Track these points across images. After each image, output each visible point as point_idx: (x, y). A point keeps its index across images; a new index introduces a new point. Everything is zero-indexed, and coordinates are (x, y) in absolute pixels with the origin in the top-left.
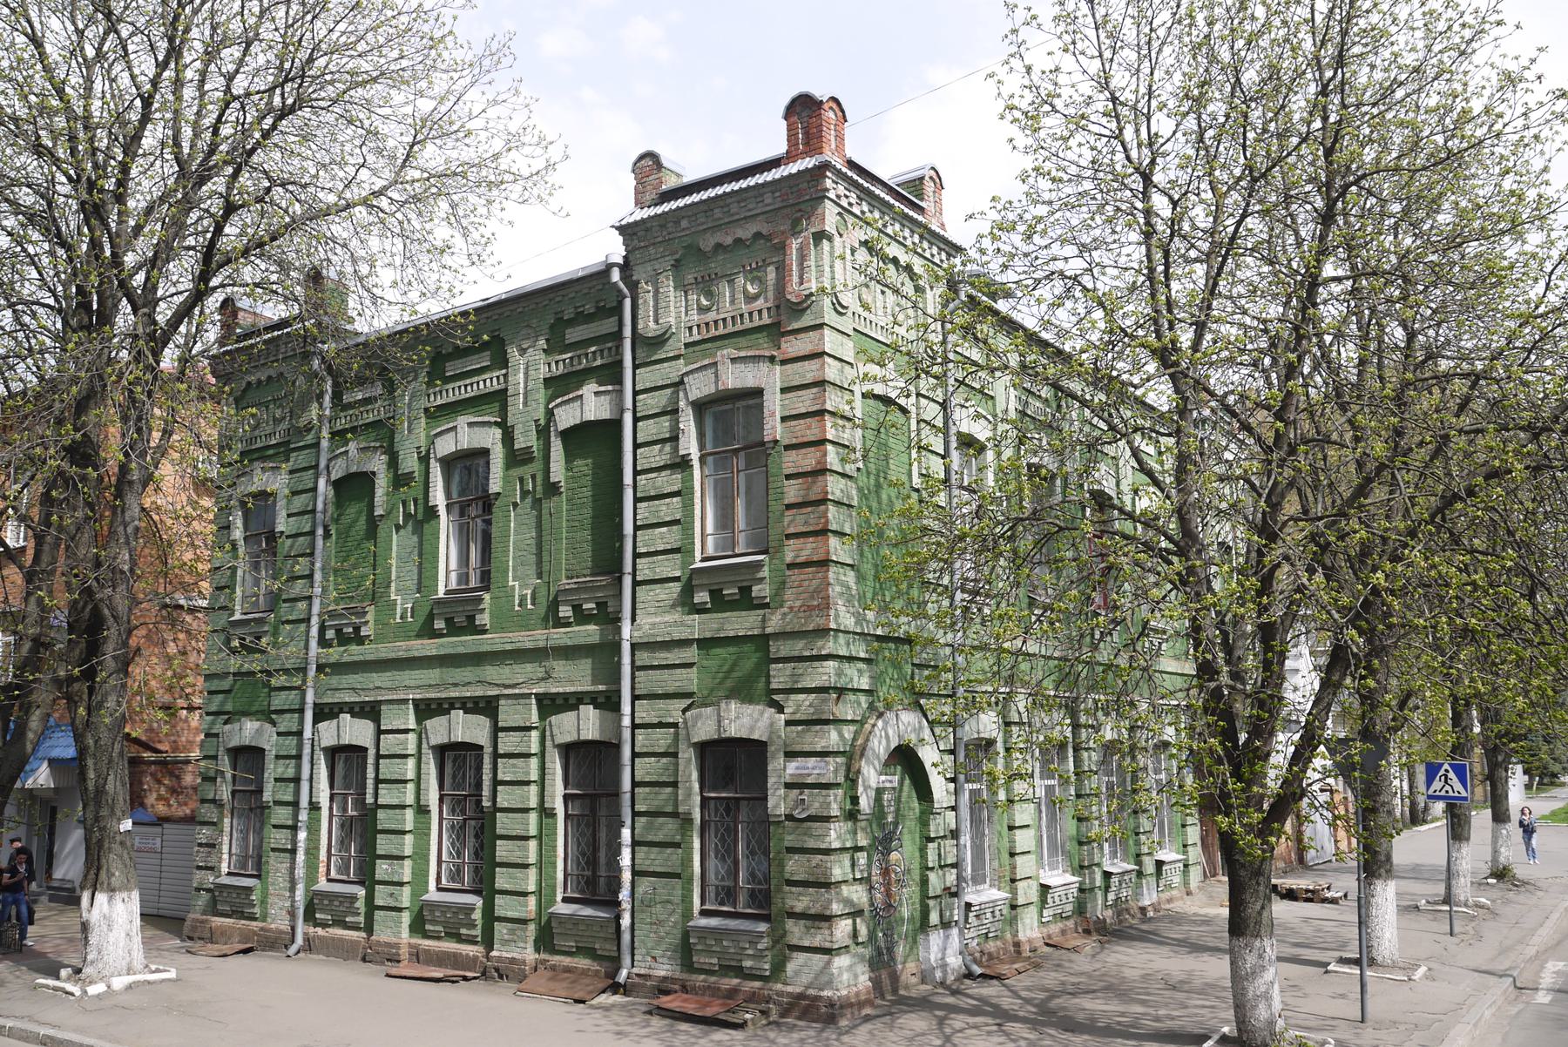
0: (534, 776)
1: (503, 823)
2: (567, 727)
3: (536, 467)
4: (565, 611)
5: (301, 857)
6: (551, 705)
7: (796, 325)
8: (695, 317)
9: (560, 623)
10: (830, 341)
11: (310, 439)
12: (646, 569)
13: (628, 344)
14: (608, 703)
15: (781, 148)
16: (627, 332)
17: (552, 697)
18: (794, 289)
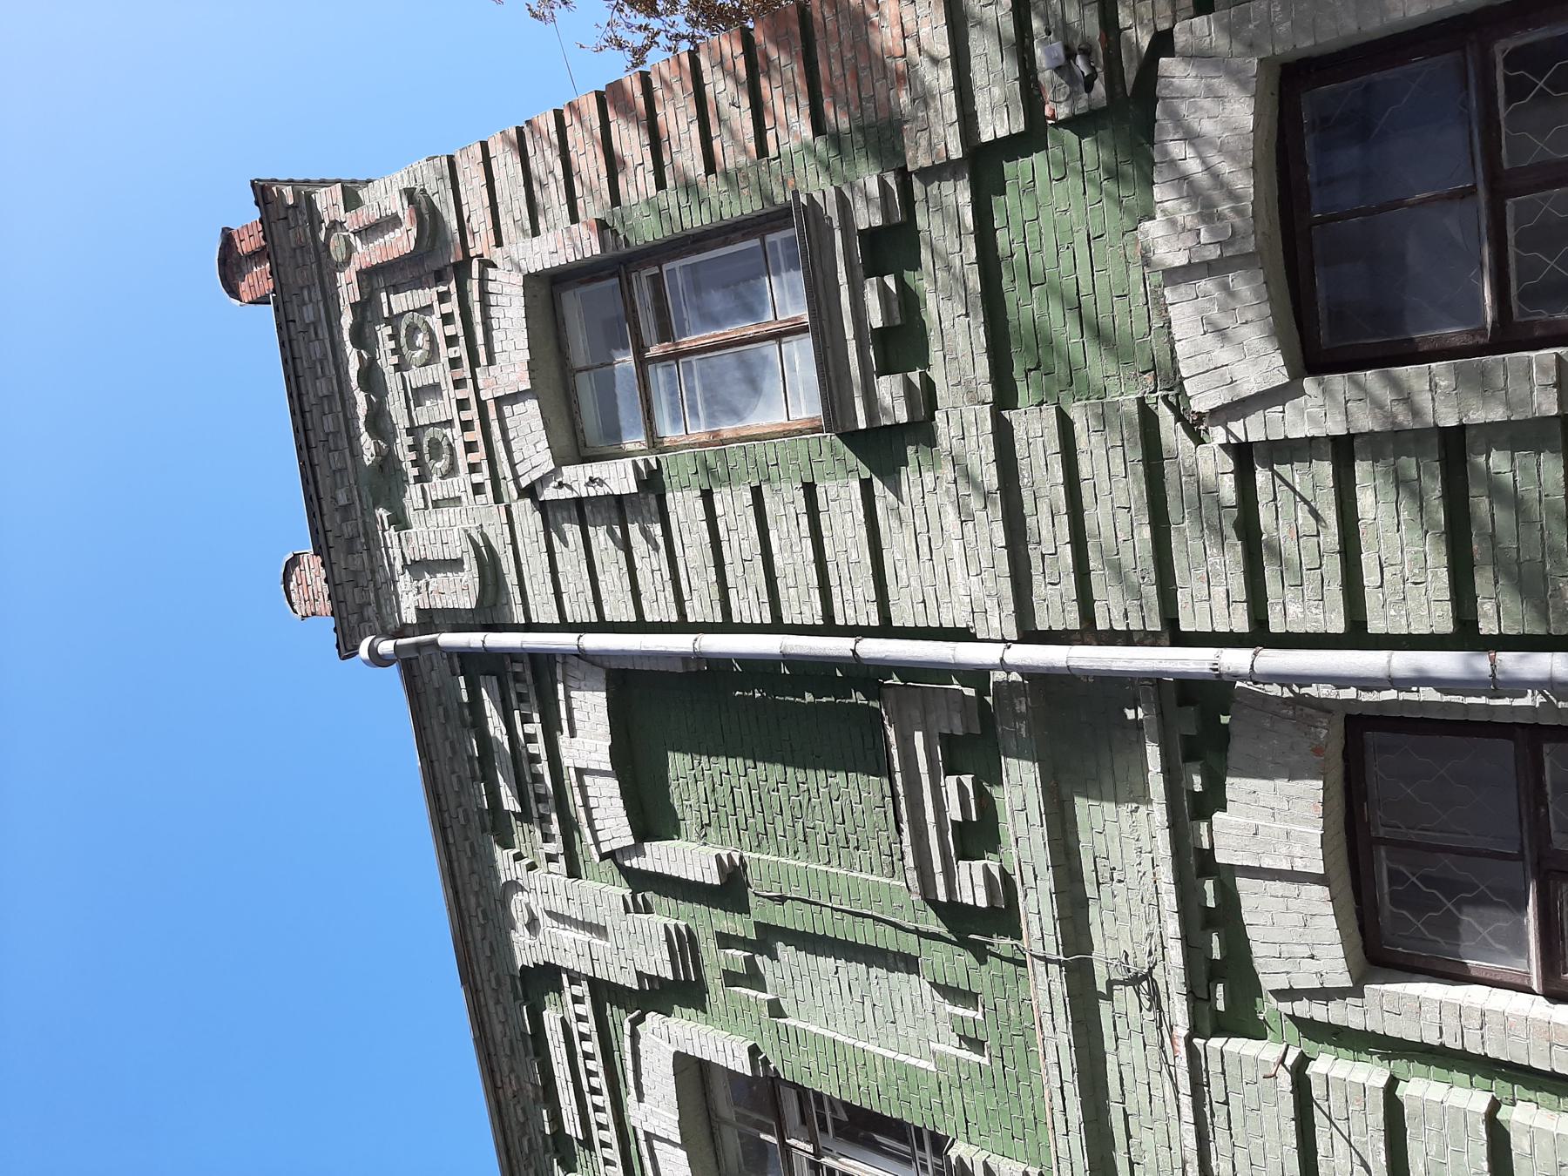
9: (1002, 914)
13: (497, 640)
16: (474, 639)
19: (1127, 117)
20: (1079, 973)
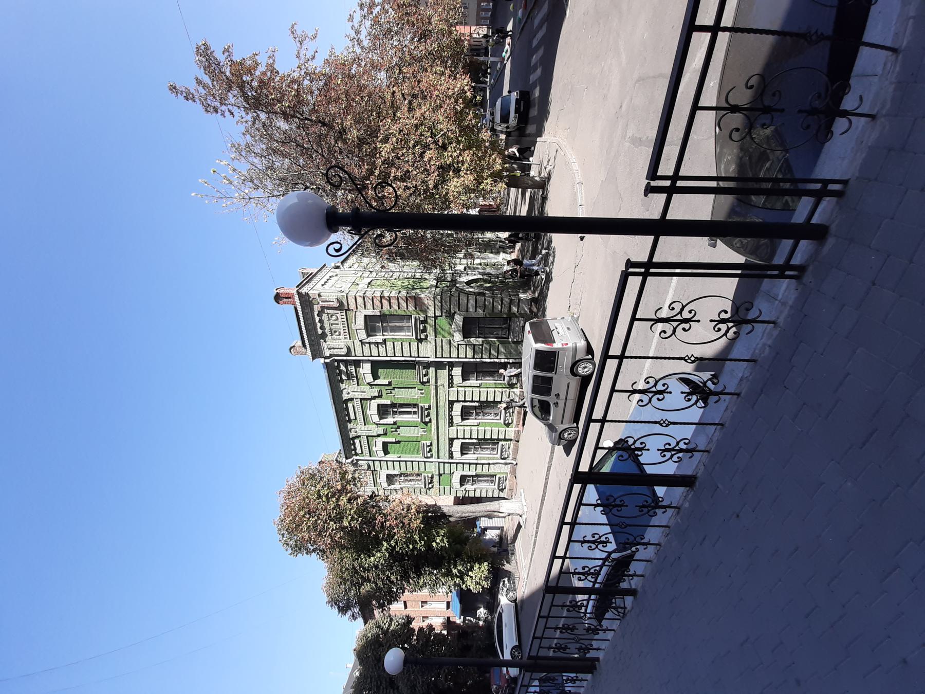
0: (470, 389)
1: (483, 399)
2: (457, 379)
3: (383, 388)
4: (425, 379)
5: (491, 462)
6: (451, 384)
7: (346, 304)
8: (342, 337)
9: (428, 382)
10: (352, 294)
11: (371, 463)
12: (414, 354)
14: (452, 365)
15: (292, 307)
17: (449, 383)
18: (336, 304)
19: (451, 316)
20: (437, 387)
